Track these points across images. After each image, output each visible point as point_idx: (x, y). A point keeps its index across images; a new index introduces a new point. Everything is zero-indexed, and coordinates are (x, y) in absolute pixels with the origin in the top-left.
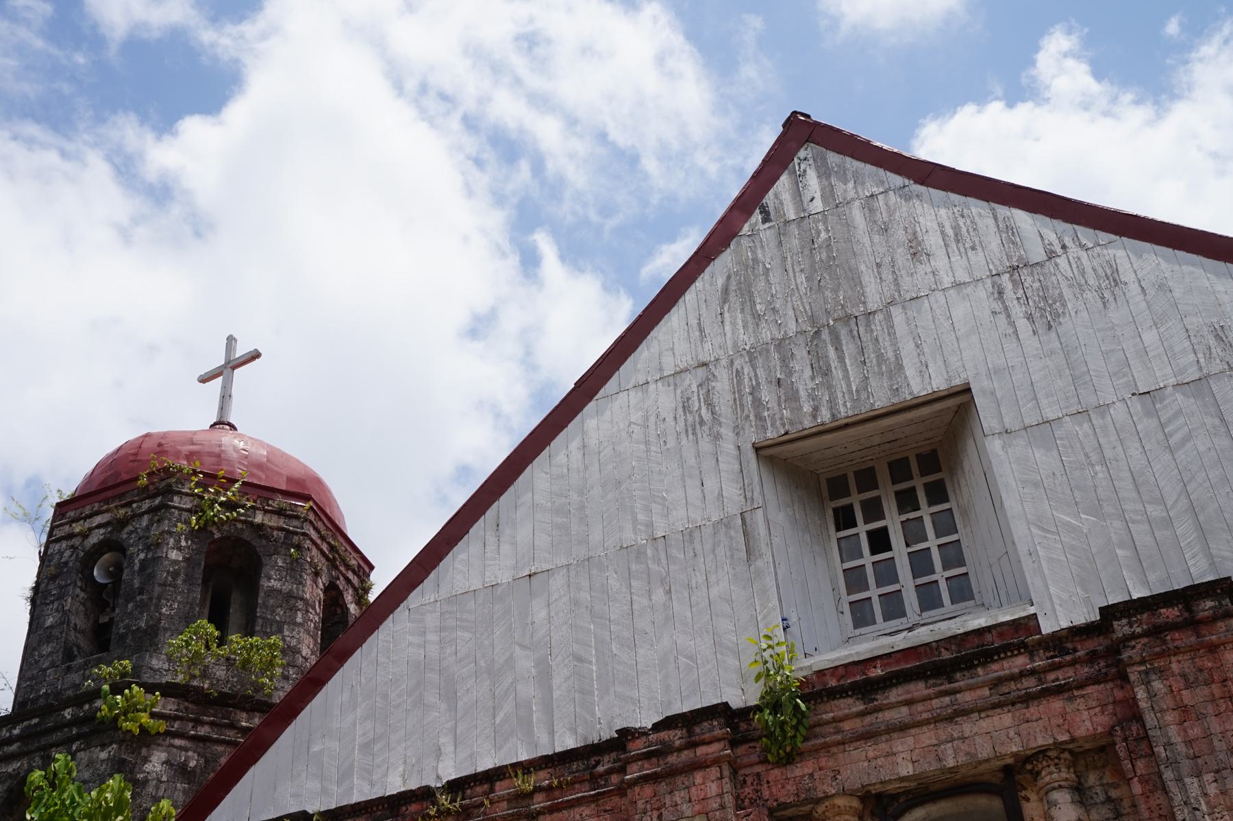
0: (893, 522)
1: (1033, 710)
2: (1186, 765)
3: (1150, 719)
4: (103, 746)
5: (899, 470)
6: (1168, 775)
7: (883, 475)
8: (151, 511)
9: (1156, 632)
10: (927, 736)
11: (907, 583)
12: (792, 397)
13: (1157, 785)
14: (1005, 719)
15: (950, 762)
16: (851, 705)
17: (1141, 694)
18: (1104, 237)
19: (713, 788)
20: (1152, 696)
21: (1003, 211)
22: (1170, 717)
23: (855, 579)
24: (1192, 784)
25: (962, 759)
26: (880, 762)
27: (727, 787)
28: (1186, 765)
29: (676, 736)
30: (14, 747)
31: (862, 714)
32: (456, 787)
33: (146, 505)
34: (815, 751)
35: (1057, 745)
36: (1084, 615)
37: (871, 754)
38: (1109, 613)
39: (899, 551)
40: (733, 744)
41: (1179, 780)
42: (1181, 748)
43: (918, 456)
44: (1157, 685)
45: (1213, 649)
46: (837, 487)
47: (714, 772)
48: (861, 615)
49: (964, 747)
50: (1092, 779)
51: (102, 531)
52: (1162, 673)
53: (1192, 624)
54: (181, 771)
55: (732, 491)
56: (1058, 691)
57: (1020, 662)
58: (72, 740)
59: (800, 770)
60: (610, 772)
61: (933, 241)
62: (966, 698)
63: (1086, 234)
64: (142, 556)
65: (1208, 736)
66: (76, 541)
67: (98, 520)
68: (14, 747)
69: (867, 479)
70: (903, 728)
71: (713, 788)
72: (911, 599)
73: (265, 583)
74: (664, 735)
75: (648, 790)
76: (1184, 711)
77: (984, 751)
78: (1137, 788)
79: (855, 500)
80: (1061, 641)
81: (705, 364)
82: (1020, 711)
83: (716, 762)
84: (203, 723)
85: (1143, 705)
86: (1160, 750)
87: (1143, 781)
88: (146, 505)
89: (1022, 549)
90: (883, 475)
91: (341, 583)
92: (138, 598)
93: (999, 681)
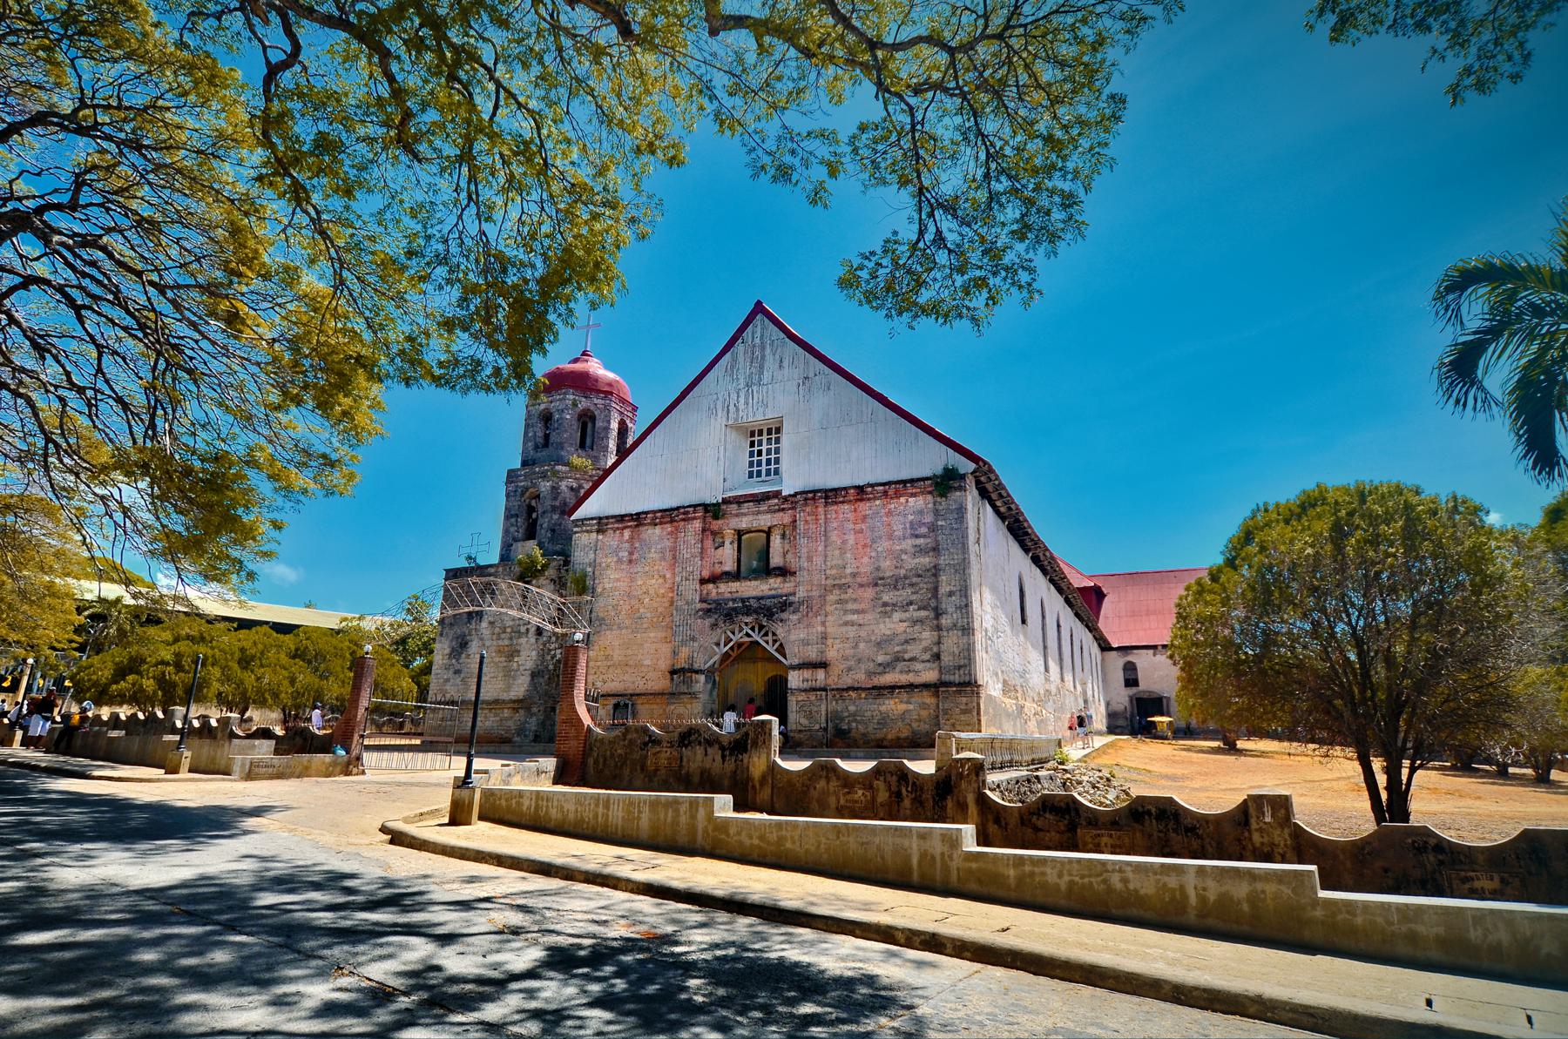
0: (764, 448)
5: (769, 432)
7: (765, 433)
9: (806, 499)
10: (751, 518)
11: (764, 468)
12: (738, 410)
14: (769, 516)
16: (735, 506)
29: (691, 509)
32: (638, 514)
38: (796, 494)
39: (764, 458)
54: (572, 489)
56: (783, 509)
59: (720, 522)
69: (760, 433)
72: (764, 472)
79: (756, 438)
80: (786, 499)
90: (765, 433)
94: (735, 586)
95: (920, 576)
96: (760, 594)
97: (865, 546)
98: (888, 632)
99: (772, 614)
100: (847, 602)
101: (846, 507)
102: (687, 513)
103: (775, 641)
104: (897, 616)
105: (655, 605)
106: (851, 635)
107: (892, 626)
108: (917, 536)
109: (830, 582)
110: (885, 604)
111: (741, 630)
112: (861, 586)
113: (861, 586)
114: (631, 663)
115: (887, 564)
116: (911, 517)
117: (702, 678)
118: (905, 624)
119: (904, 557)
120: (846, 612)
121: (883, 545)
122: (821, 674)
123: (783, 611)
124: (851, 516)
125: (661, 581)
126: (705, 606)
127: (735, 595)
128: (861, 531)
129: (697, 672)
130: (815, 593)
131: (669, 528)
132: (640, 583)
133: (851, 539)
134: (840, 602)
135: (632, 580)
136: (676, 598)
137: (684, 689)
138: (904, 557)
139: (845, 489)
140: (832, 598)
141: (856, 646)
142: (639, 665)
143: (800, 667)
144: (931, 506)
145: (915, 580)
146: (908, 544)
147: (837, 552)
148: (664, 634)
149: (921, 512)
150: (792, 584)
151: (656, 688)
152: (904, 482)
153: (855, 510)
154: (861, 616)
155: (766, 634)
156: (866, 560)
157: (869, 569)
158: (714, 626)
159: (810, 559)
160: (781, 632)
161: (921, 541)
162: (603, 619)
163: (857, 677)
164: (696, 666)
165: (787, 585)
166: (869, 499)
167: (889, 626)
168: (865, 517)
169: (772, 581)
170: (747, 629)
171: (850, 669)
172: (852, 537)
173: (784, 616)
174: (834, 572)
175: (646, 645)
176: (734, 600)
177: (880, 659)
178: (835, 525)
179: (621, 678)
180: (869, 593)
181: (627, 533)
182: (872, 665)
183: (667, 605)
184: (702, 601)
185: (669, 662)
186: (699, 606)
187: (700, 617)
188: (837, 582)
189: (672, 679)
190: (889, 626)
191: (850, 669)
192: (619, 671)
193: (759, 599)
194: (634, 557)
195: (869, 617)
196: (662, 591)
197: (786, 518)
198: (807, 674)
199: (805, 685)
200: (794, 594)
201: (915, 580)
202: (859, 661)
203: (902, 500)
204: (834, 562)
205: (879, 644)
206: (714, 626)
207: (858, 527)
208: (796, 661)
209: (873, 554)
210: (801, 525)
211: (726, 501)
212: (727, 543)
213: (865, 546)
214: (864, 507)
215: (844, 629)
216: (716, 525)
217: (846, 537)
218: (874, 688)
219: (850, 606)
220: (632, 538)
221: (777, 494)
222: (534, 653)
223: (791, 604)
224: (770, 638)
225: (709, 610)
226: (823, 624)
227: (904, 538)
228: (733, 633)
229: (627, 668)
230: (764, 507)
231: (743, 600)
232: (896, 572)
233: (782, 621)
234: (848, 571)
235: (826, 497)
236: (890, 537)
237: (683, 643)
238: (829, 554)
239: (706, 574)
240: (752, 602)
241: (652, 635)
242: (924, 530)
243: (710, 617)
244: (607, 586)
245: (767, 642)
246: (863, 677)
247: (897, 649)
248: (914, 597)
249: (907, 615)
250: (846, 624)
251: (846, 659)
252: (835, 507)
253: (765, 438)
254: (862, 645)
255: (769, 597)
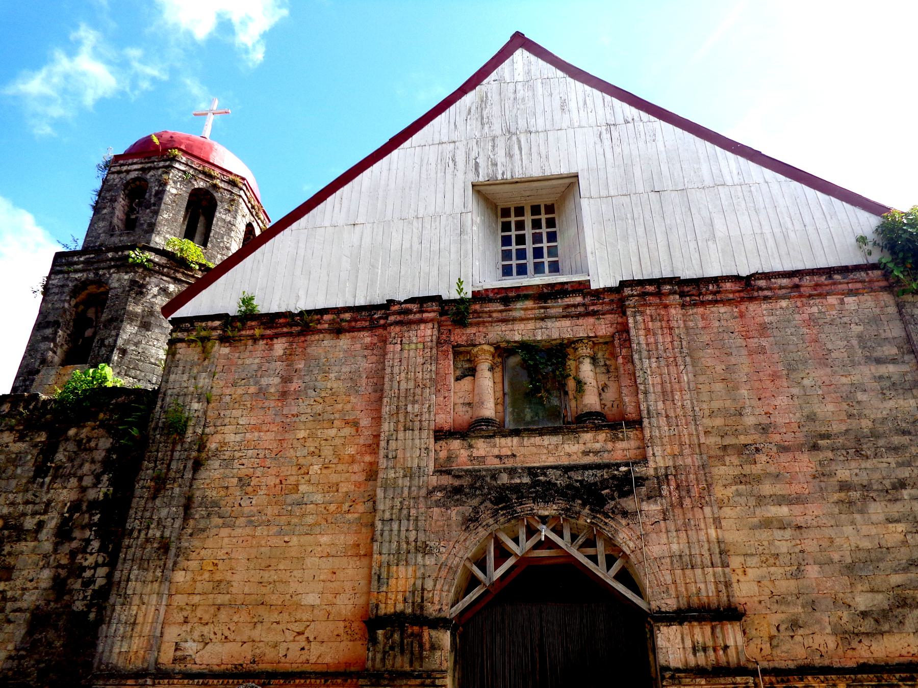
1: (581, 321)
2: (645, 354)
3: (633, 332)
4: (127, 273)
5: (536, 210)
6: (636, 356)
7: (528, 211)
8: (164, 167)
9: (643, 295)
10: (531, 325)
13: (630, 360)
14: (567, 323)
15: (539, 338)
17: (631, 320)
18: (652, 118)
19: (429, 332)
20: (636, 322)
21: (608, 98)
22: (642, 332)
23: (506, 255)
24: (646, 362)
25: (545, 337)
26: (507, 333)
27: (436, 332)
28: (645, 354)
29: (414, 307)
30: (80, 266)
31: (501, 311)
33: (161, 164)
34: (478, 324)
35: (589, 337)
36: (613, 282)
37: (503, 329)
38: (623, 284)
40: (441, 315)
41: (641, 359)
42: (644, 346)
43: (546, 206)
44: (639, 318)
45: (666, 307)
46: (506, 212)
47: (430, 325)
48: (507, 271)
49: (547, 332)
50: (600, 355)
51: (137, 172)
52: (642, 313)
53: (659, 294)
55: (459, 201)
56: (594, 314)
57: (579, 299)
58: (110, 268)
59: (471, 330)
60: (380, 318)
61: (573, 105)
62: (552, 311)
63: (645, 116)
64: (157, 188)
65: (656, 343)
66: (123, 176)
67: (135, 167)
68: (80, 266)
69: (520, 211)
70: (522, 320)
71: (429, 332)
72: (530, 268)
73: (217, 214)
74: (409, 306)
75: (398, 329)
76: (647, 330)
77: (555, 335)
78: (620, 360)
79: (513, 219)
80: (598, 293)
81: (454, 142)
82: (575, 321)
83: (432, 320)
84: (178, 272)
85: (631, 325)
86: (634, 346)
87: (624, 358)
88: (161, 164)
89: (589, 250)
90: (528, 211)
91: (255, 224)
92: (153, 208)
93: (568, 306)
94: (507, 445)
95: (904, 433)
96: (565, 462)
97: (774, 377)
98: (866, 544)
99: (602, 501)
100: (758, 479)
101: (723, 309)
102: (408, 312)
103: (610, 561)
104: (878, 510)
105: (334, 478)
106: (783, 547)
107: (873, 531)
108: (879, 361)
109: (712, 440)
110: (844, 487)
111: (531, 532)
112: (784, 449)
113: (784, 449)
114: (274, 599)
115: (827, 409)
116: (857, 329)
117: (445, 638)
118: (901, 527)
119: (860, 396)
120: (761, 500)
121: (813, 376)
122: (732, 635)
123: (625, 494)
124: (735, 324)
125: (347, 431)
126: (446, 480)
127: (509, 464)
128: (762, 350)
129: (439, 623)
130: (689, 460)
131: (367, 338)
132: (301, 434)
133: (743, 363)
134: (741, 479)
135: (286, 428)
136: (383, 463)
137: (402, 663)
138: (860, 396)
139: (716, 280)
140: (724, 471)
141: (798, 573)
142: (289, 606)
143: (680, 617)
144: (892, 310)
145: (897, 440)
146: (865, 373)
147: (719, 387)
148: (351, 539)
149: (875, 320)
150: (633, 444)
151: (328, 659)
152: (829, 272)
153: (742, 315)
154: (797, 509)
155: (590, 543)
156: (782, 401)
157: (795, 418)
158: (471, 522)
159: (666, 395)
160: (625, 537)
161: (884, 370)
162: (215, 504)
163: (819, 640)
164: (431, 610)
165: (620, 445)
166: (766, 298)
167: (865, 530)
168: (763, 329)
169: (587, 436)
170: (545, 532)
171: (794, 625)
172: (745, 360)
173: (629, 504)
174: (719, 422)
175: (309, 561)
176: (512, 472)
177: (862, 601)
178: (705, 338)
179: (247, 633)
180: (805, 464)
181: (280, 346)
182: (846, 616)
183: (361, 477)
184: (439, 471)
185: (361, 601)
186: (434, 481)
187: (438, 504)
188: (728, 441)
189: (373, 640)
190: (865, 530)
191: (794, 625)
192: (243, 617)
193: (567, 469)
194: (293, 386)
195: (814, 511)
196: (351, 450)
197: (603, 327)
198: (701, 633)
199: (701, 659)
200: (644, 460)
201: (897, 440)
202: (813, 605)
203: (832, 300)
204: (715, 405)
205: (850, 569)
206: (471, 522)
207: (753, 343)
208: (669, 604)
209: (795, 391)
210: (639, 337)
211: (479, 297)
212: (484, 368)
213: (774, 377)
214: (758, 311)
215: (764, 535)
216: (460, 336)
217: (733, 360)
218: (864, 668)
219: (767, 489)
220: (288, 356)
221: (582, 288)
222: (46, 574)
223: (641, 481)
224: (601, 549)
225: (458, 490)
226: (717, 522)
227: (853, 364)
228: (516, 540)
229: (261, 610)
230: (556, 306)
231: (531, 471)
232: (854, 424)
233: (625, 514)
234: (750, 420)
235: (682, 295)
236: (824, 360)
237: (401, 557)
238: (704, 388)
239: (445, 420)
240: (553, 475)
241: (324, 539)
242: (891, 350)
243: (462, 503)
244: (231, 438)
245: (594, 558)
246: (831, 642)
247: (896, 579)
248: (904, 473)
249: (898, 506)
250: (766, 524)
251: (781, 600)
252: (701, 310)
253: (528, 219)
254: (812, 571)
255: (586, 467)
